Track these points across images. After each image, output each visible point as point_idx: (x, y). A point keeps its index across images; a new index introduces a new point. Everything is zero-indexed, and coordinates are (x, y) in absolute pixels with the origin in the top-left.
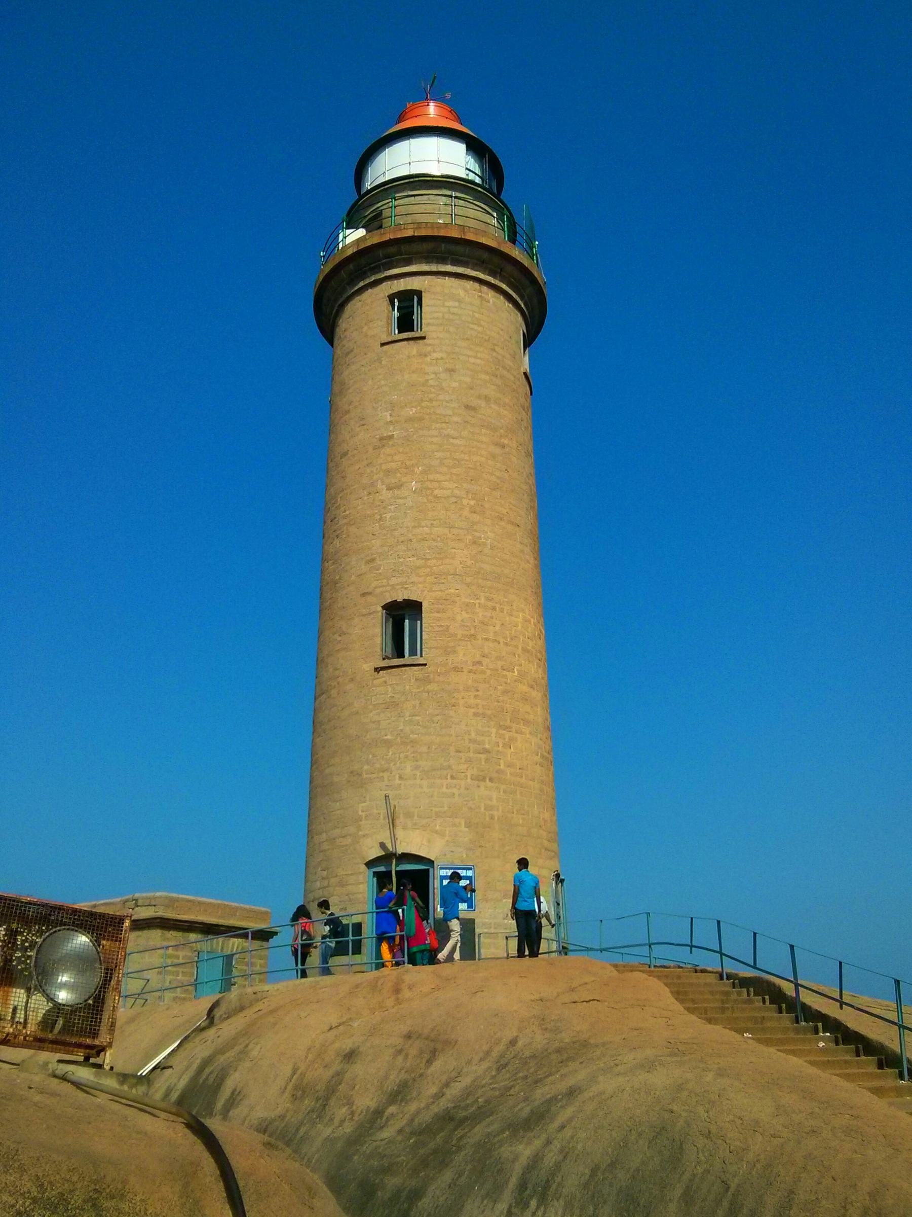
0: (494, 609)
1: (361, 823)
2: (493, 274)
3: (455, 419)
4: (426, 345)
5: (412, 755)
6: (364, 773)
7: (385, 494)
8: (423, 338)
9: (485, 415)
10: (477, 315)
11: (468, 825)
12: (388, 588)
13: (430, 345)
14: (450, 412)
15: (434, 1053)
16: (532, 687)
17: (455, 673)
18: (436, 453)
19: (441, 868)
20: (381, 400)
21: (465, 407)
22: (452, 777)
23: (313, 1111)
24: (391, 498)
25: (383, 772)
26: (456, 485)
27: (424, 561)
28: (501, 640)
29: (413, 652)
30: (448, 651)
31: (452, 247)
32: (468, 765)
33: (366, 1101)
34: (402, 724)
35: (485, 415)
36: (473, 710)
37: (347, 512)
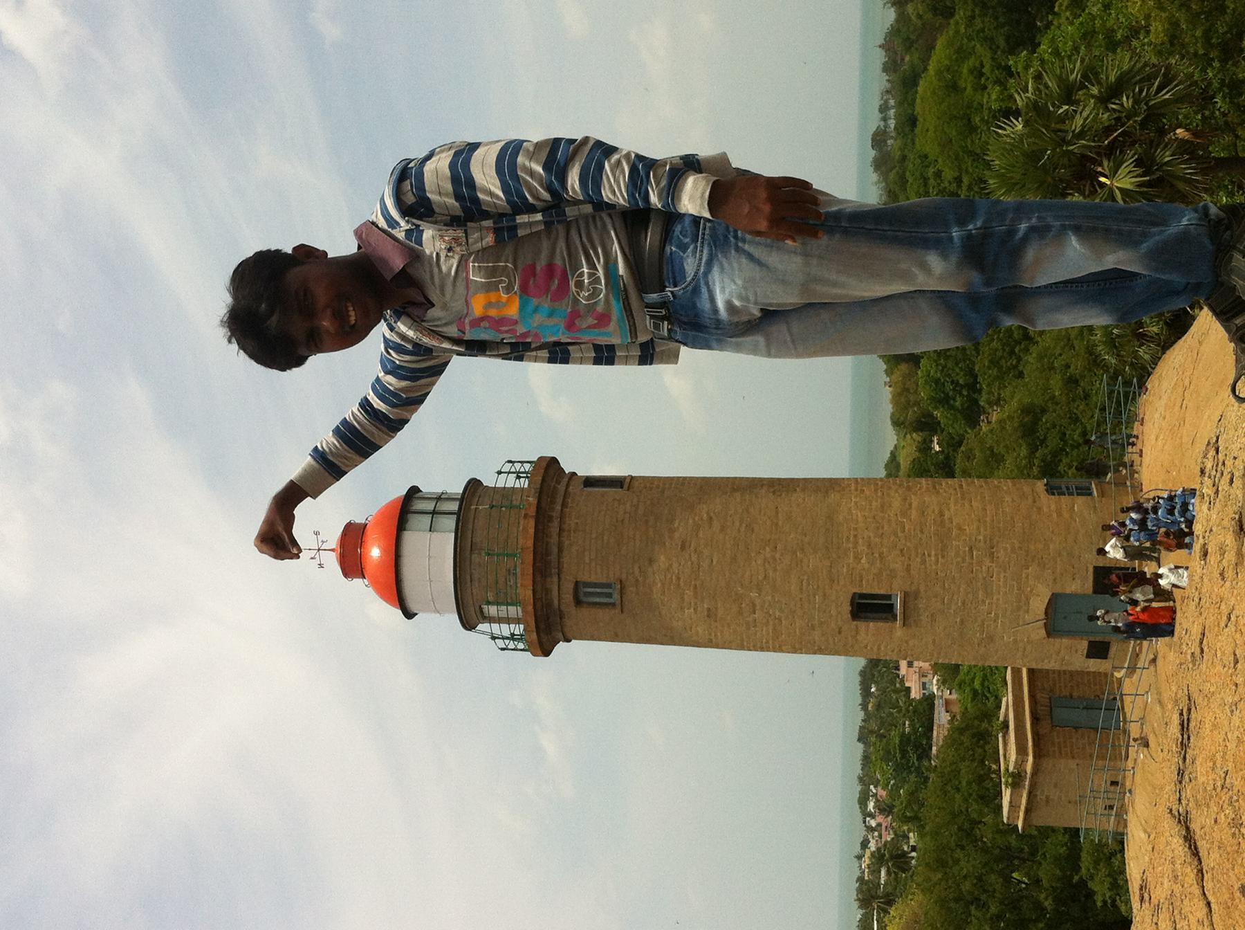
0: (855, 536)
2: (550, 519)
3: (694, 558)
14: (690, 563)
16: (910, 505)
26: (754, 562)
28: (881, 531)
29: (889, 597)
30: (893, 575)
36: (940, 559)
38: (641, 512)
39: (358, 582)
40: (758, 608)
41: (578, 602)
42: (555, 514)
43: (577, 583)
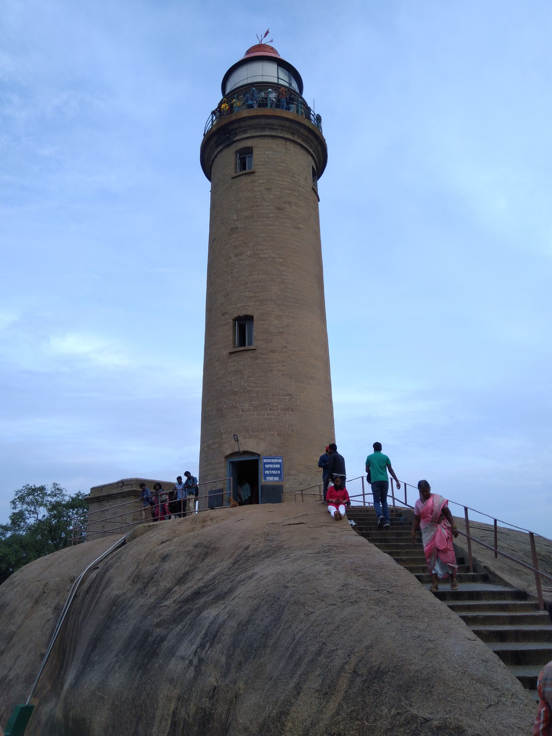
0: (294, 318)
1: (222, 436)
2: (293, 134)
3: (272, 215)
4: (256, 176)
5: (249, 398)
6: (224, 409)
7: (234, 259)
8: (253, 172)
9: (288, 212)
10: (283, 158)
11: (279, 435)
12: (236, 309)
13: (258, 176)
14: (268, 212)
15: (206, 555)
17: (271, 353)
18: (260, 235)
19: (264, 459)
20: (232, 209)
21: (277, 208)
22: (270, 410)
23: (140, 590)
24: (237, 261)
25: (233, 408)
27: (254, 294)
29: (250, 344)
31: (269, 121)
32: (279, 403)
33: (165, 584)
34: (243, 382)
35: (288, 212)
37: (216, 271)
38: (300, 189)
40: (240, 257)
42: (296, 139)
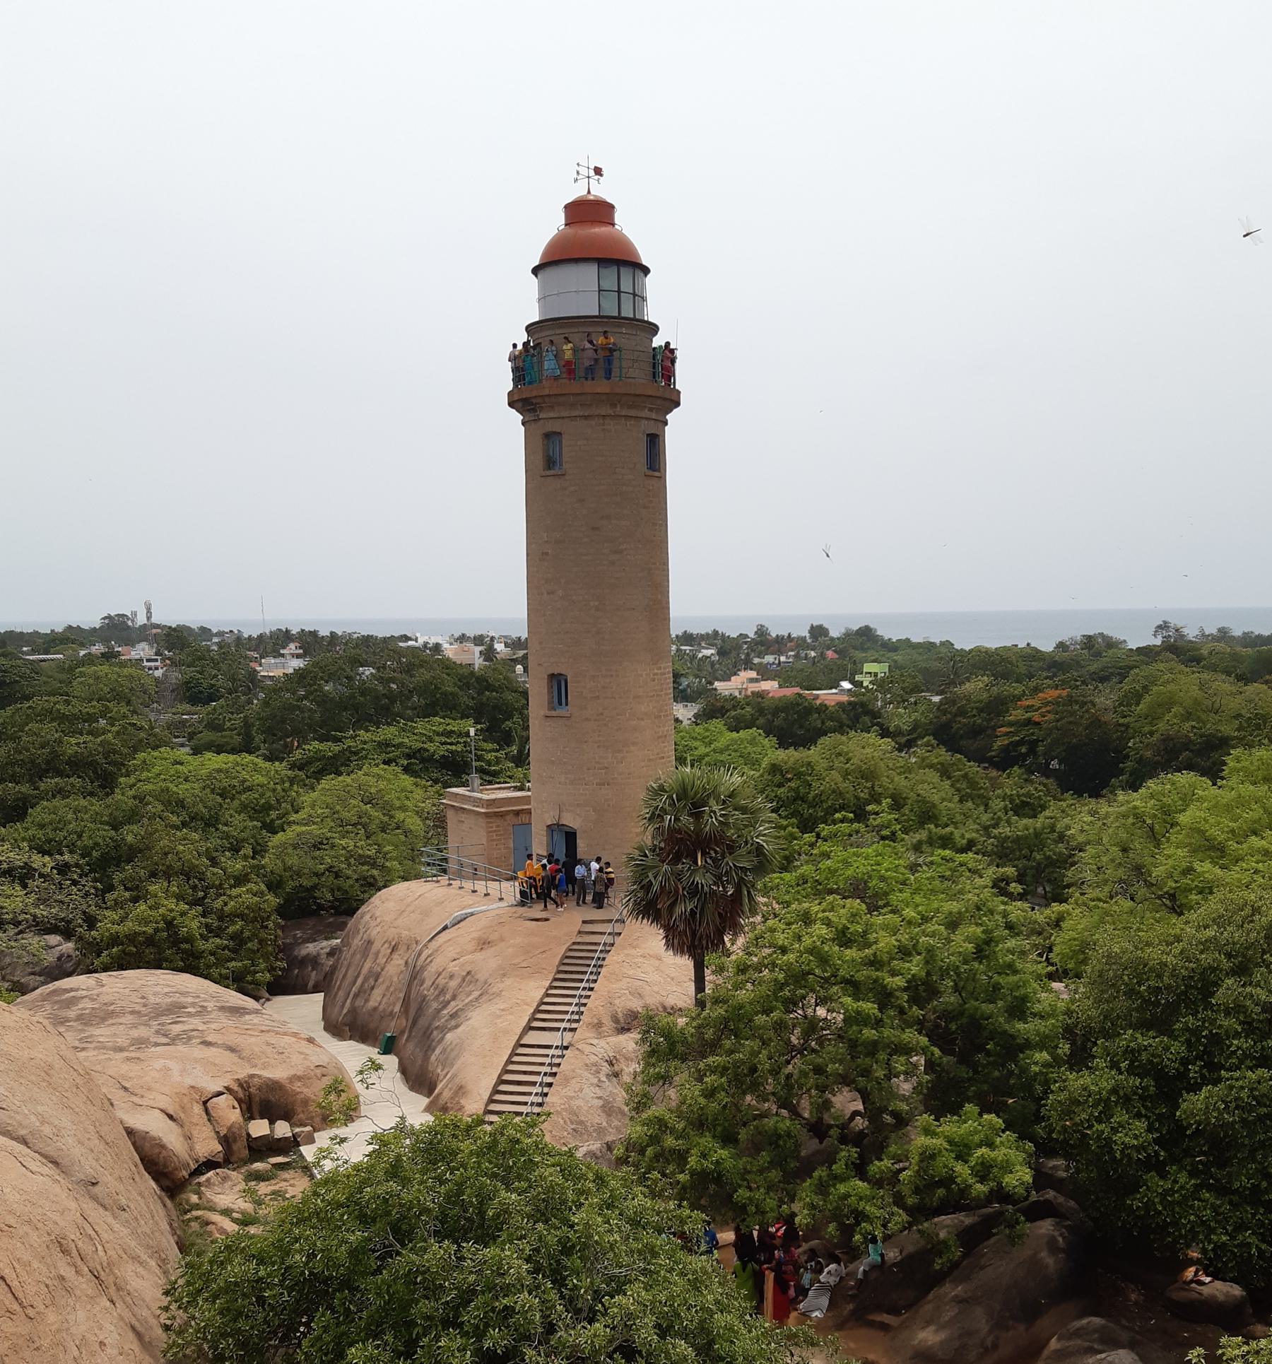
2: (613, 406)
3: (585, 540)
16: (642, 719)
29: (567, 704)
39: (560, 220)
41: (548, 436)
43: (560, 434)
